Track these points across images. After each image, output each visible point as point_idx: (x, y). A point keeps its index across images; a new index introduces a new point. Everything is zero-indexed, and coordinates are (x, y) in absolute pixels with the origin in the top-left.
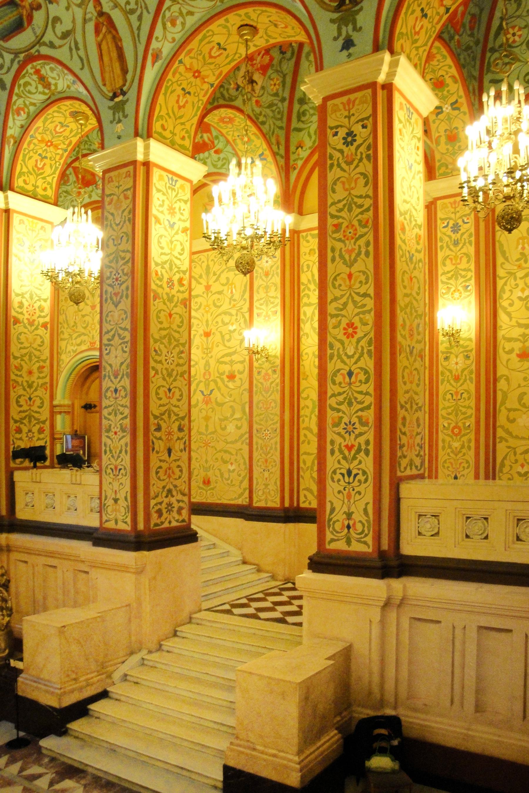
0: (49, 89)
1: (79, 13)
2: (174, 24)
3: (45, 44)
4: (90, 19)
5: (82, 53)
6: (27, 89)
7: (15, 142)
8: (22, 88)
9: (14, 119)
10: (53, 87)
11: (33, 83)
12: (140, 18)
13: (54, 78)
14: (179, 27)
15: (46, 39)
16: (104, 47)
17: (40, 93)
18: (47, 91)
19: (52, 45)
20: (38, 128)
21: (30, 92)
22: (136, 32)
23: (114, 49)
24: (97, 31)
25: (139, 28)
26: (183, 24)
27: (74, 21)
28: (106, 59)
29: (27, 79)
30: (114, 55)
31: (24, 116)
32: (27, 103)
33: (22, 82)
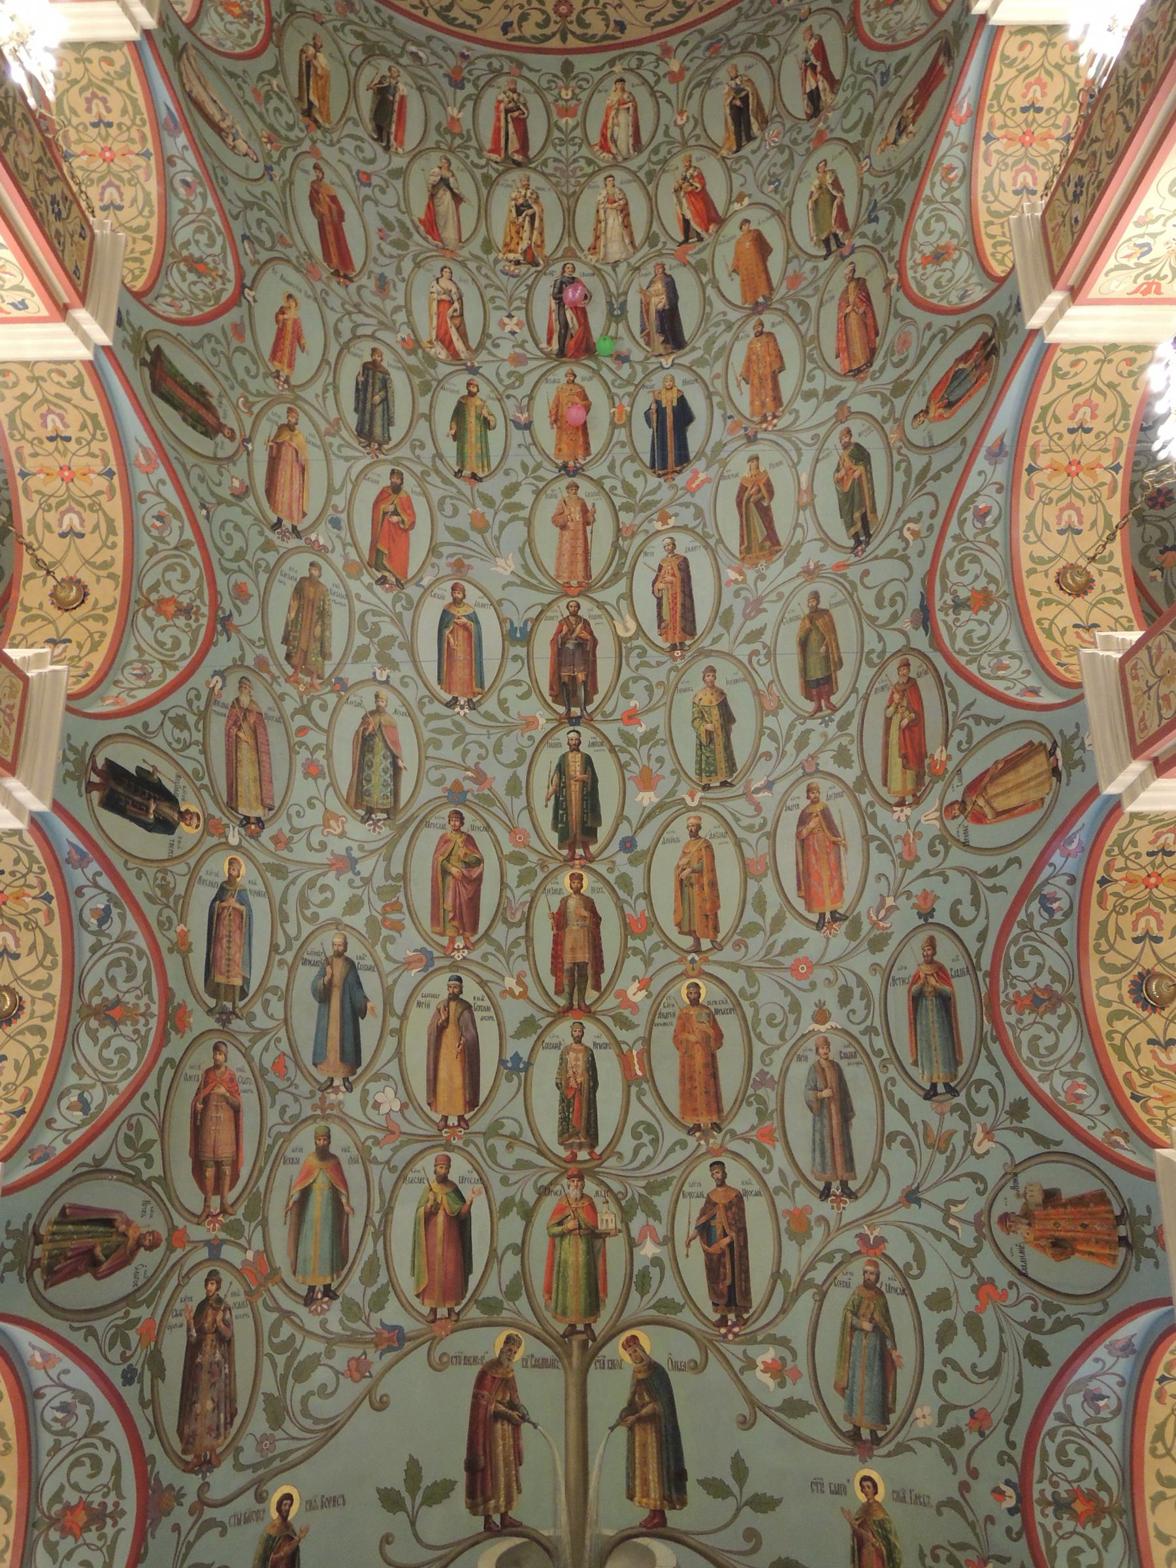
0: (1060, 1000)
1: (958, 856)
2: (1006, 667)
3: (979, 954)
4: (966, 831)
5: (1000, 861)
6: (1042, 1051)
7: (1125, 1136)
8: (1036, 1060)
9: (1081, 1113)
10: (1057, 987)
11: (1038, 1030)
12: (978, 719)
13: (1040, 967)
14: (1015, 663)
15: (973, 948)
16: (1001, 804)
17: (1061, 1027)
18: (1062, 1010)
19: (982, 937)
20: (1127, 1077)
21: (1052, 1049)
22: (993, 728)
23: (1005, 778)
24: (979, 818)
25: (989, 721)
26: (1013, 656)
27: (962, 871)
28: (1014, 800)
29: (1025, 1037)
30: (1011, 778)
31: (1087, 1092)
32: (1068, 1068)
33: (1026, 1053)
